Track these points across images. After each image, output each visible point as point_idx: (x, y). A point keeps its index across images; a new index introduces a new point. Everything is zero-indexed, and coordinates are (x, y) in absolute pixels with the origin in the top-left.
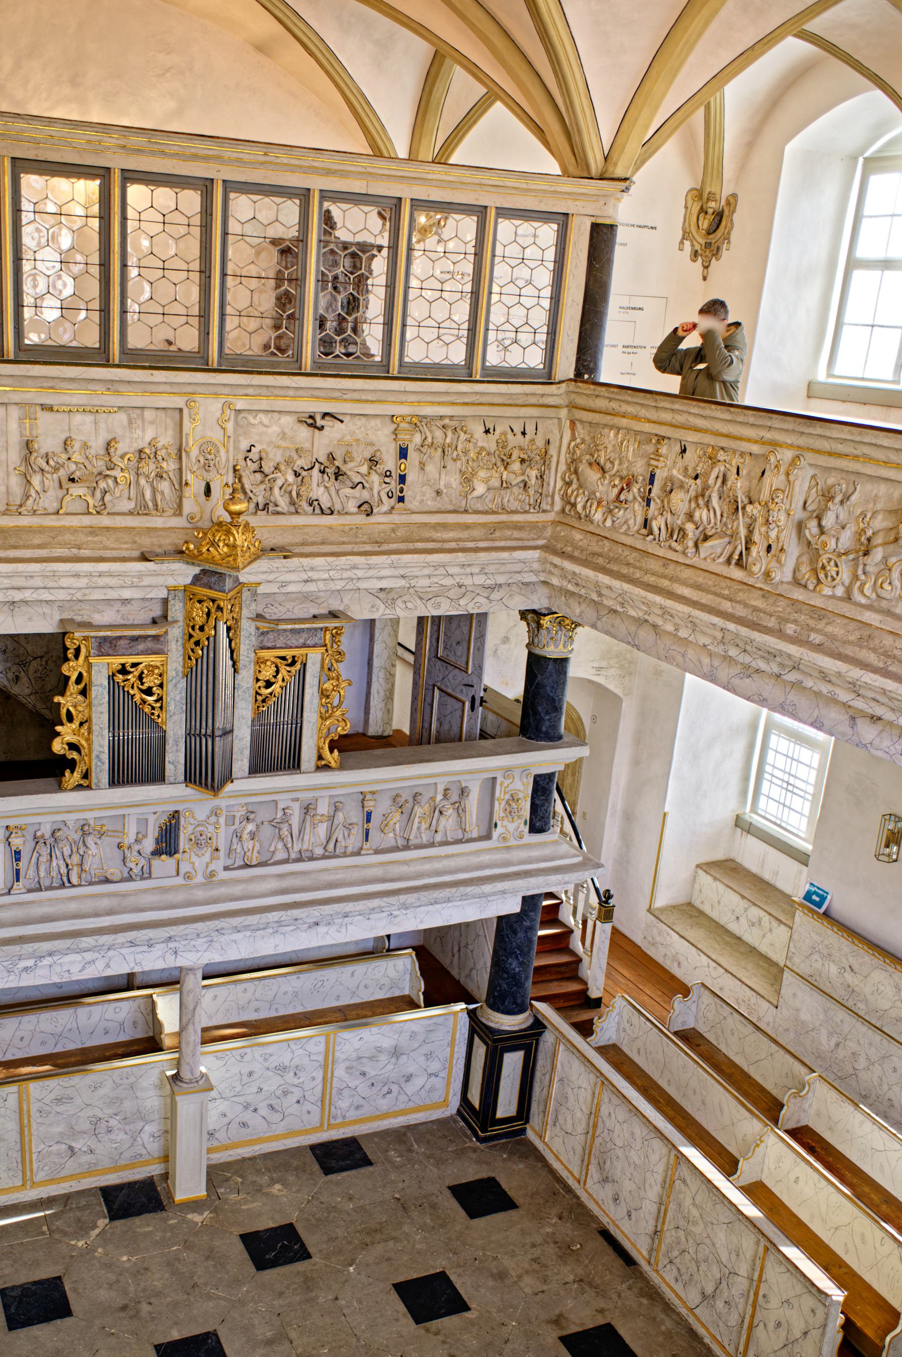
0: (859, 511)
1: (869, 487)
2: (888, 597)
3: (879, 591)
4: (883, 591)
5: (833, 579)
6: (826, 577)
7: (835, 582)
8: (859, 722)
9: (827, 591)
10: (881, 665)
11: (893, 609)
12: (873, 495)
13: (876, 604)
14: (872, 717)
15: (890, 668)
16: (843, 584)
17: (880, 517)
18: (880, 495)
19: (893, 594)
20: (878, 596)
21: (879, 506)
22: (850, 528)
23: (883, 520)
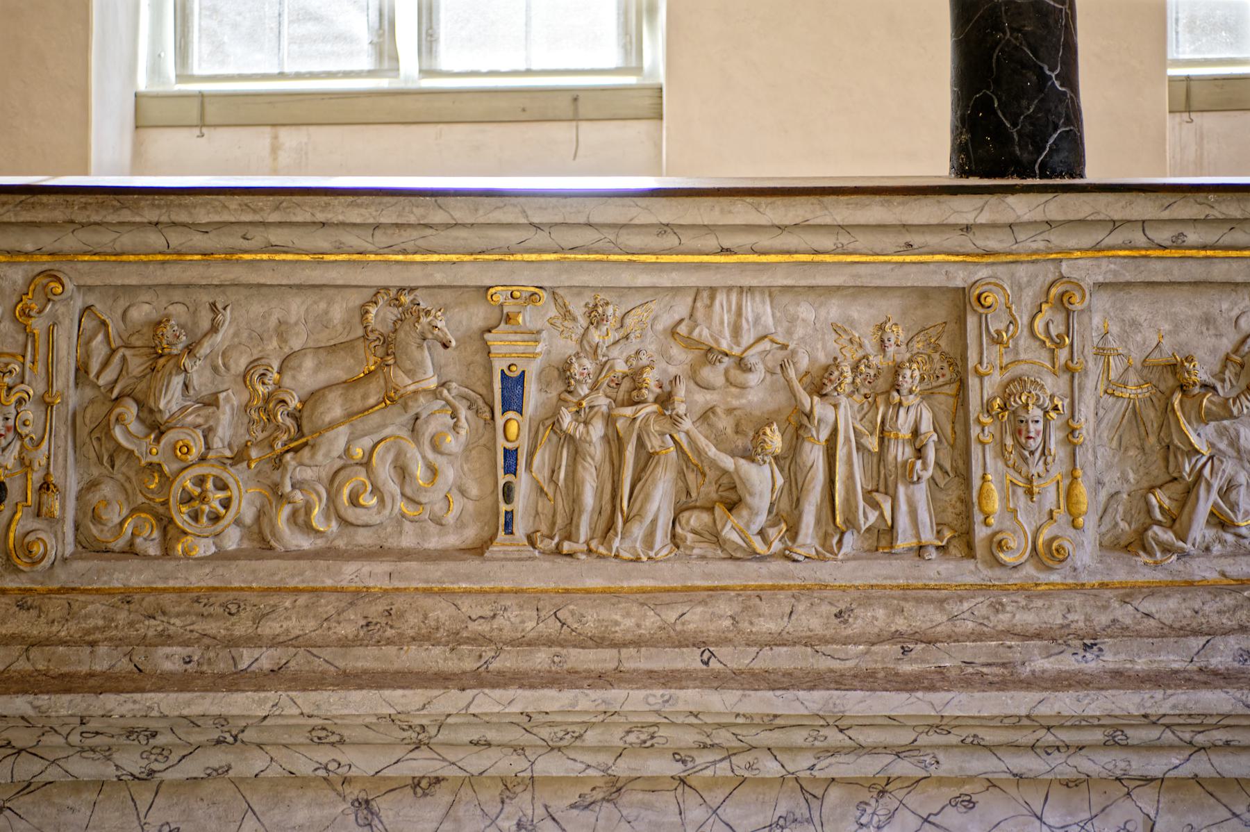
0: (243, 362)
1: (256, 308)
2: (376, 519)
3: (351, 514)
4: (358, 510)
5: (216, 518)
6: (195, 517)
7: (223, 523)
8: (384, 806)
9: (204, 548)
10: (469, 665)
11: (392, 543)
12: (273, 322)
13: (341, 543)
14: (416, 783)
15: (495, 665)
16: (238, 522)
17: (309, 363)
18: (293, 320)
19: (387, 512)
20: (344, 522)
21: (296, 344)
22: (227, 399)
23: (317, 368)
